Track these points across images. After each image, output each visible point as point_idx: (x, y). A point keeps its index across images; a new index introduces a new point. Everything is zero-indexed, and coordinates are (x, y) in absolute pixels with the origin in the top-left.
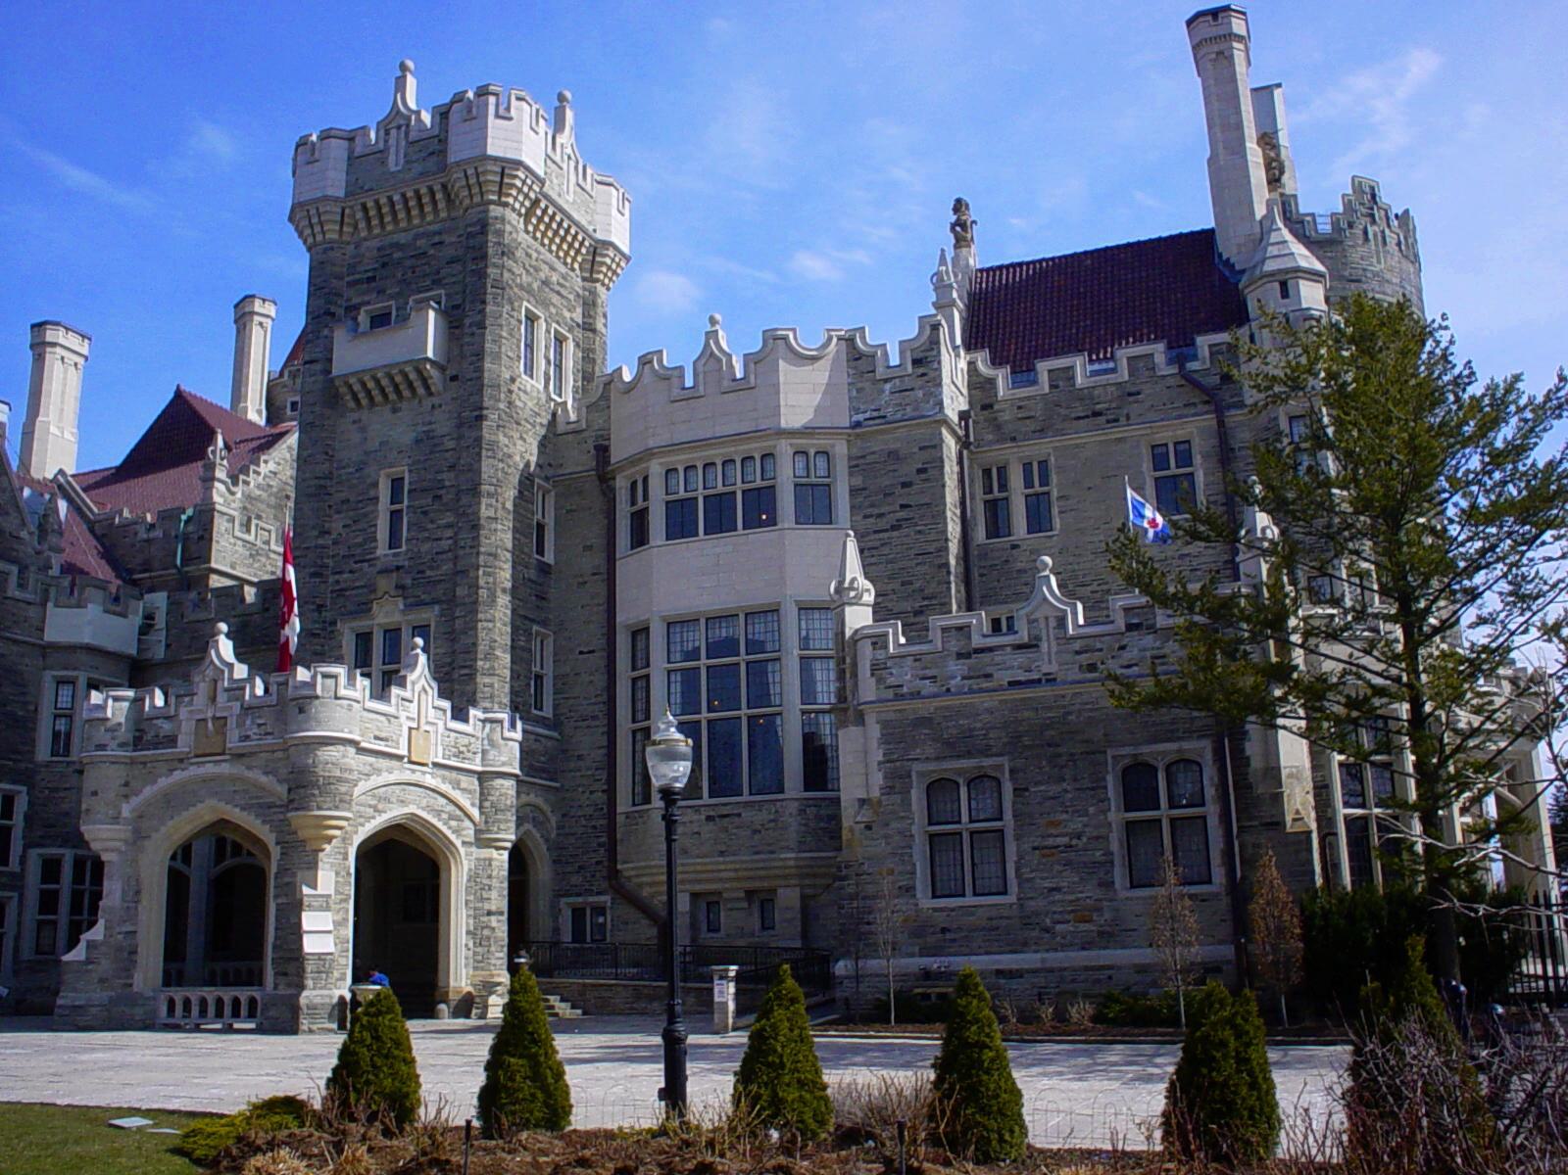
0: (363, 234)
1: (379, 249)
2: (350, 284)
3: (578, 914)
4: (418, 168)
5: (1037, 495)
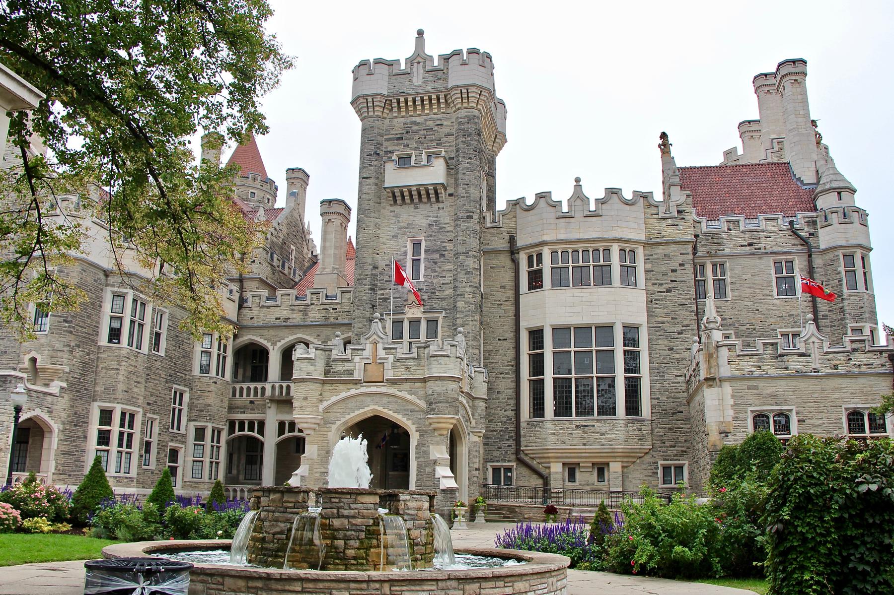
0: (396, 115)
1: (404, 124)
2: (387, 140)
3: (496, 470)
4: (432, 85)
5: (719, 280)
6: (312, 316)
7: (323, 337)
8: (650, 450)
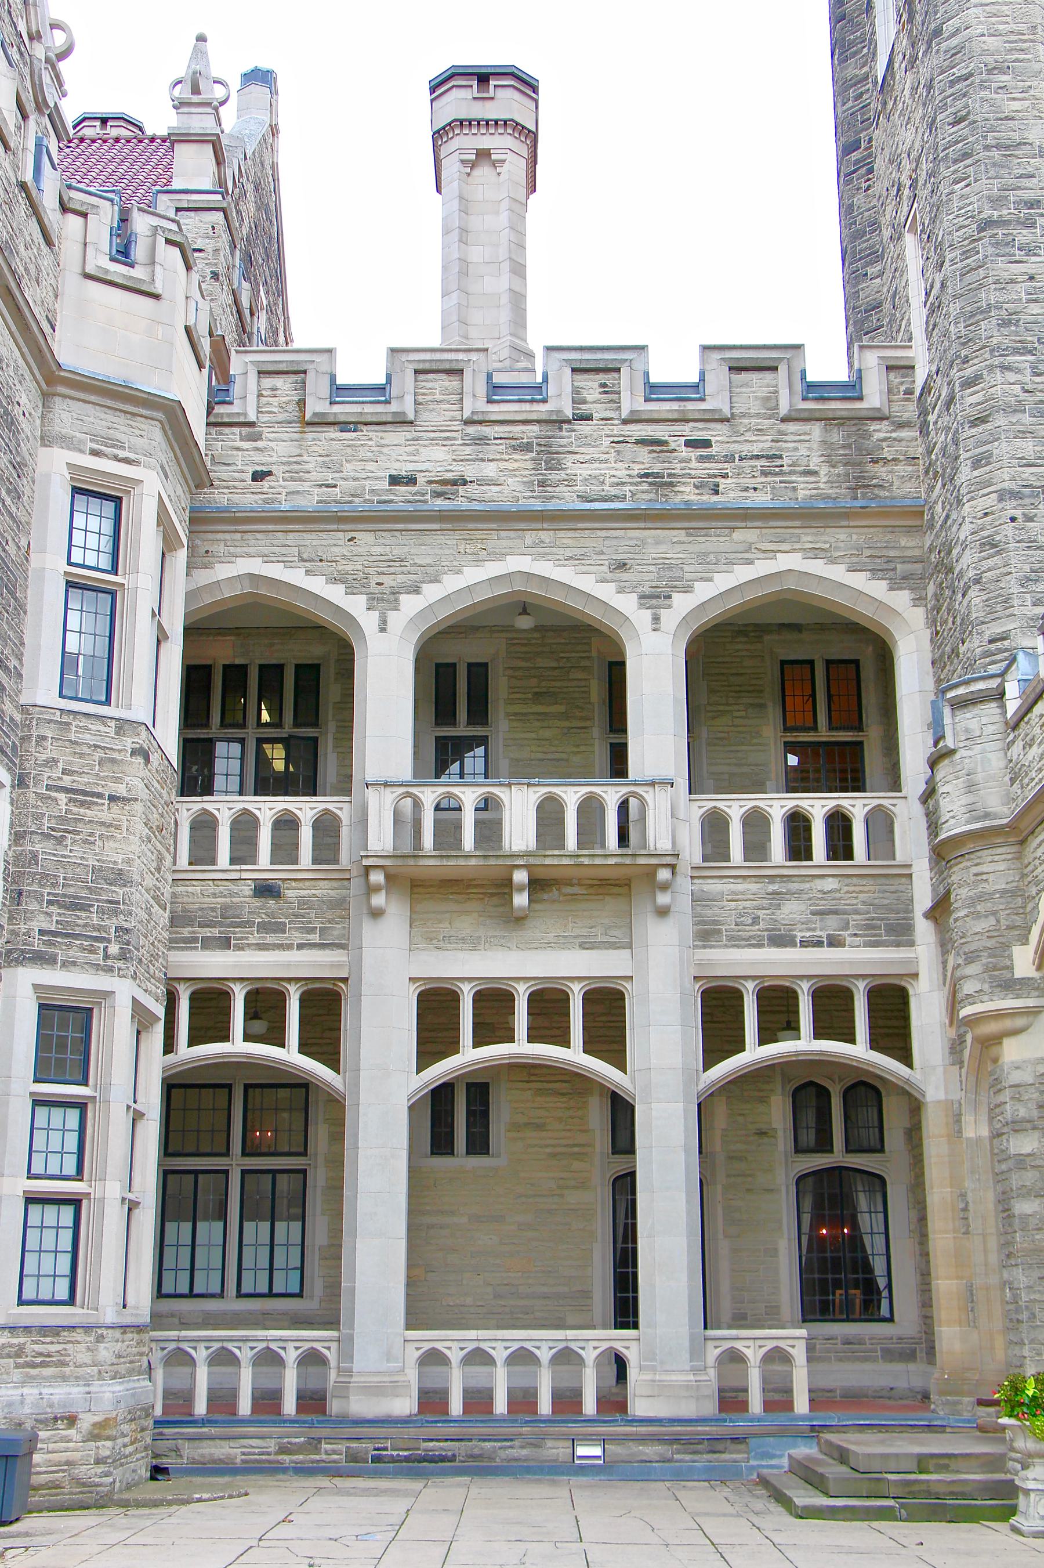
6: (583, 471)
7: (646, 575)
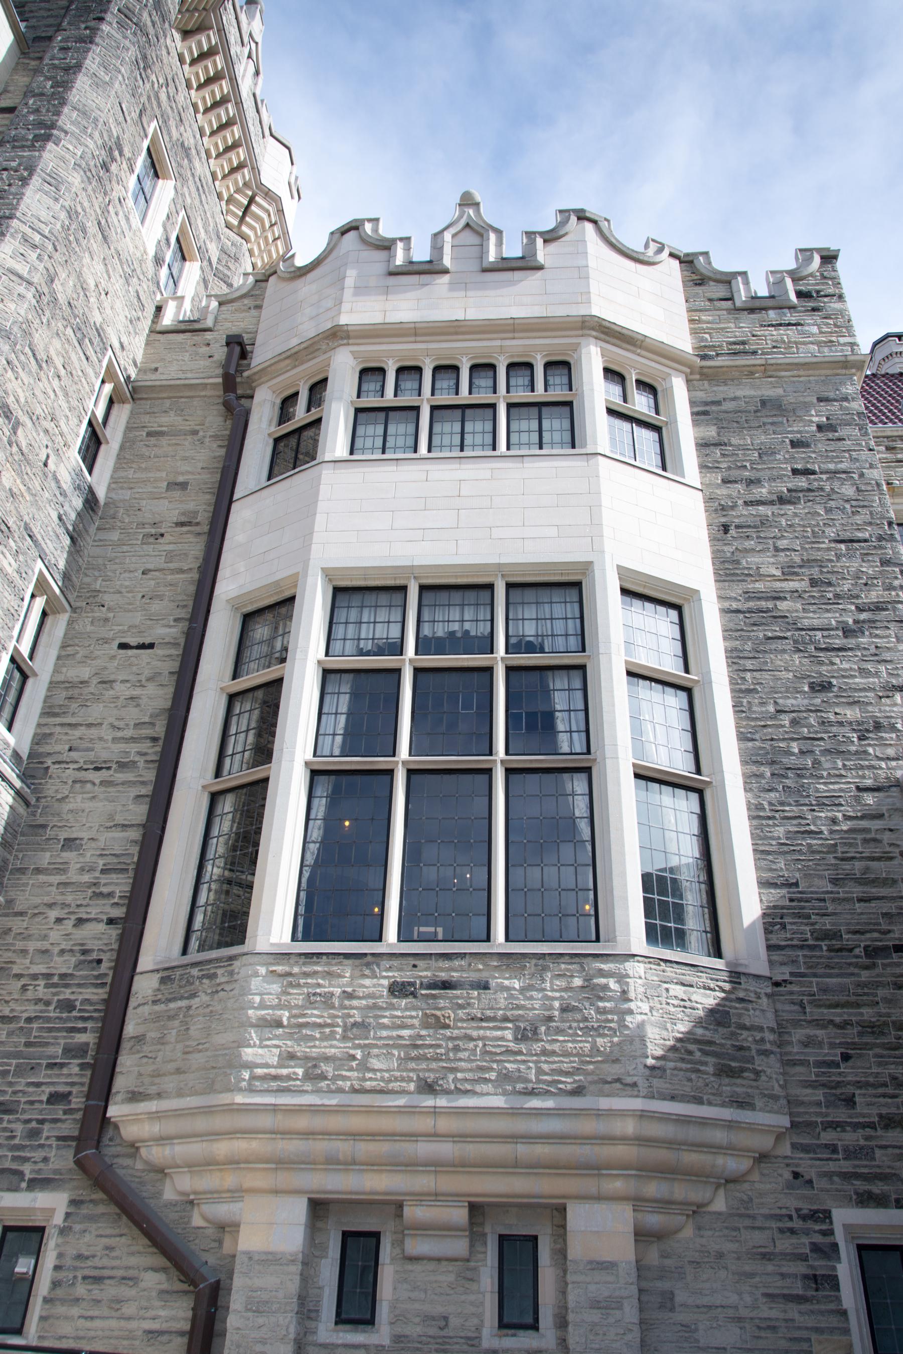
8: (779, 1137)
